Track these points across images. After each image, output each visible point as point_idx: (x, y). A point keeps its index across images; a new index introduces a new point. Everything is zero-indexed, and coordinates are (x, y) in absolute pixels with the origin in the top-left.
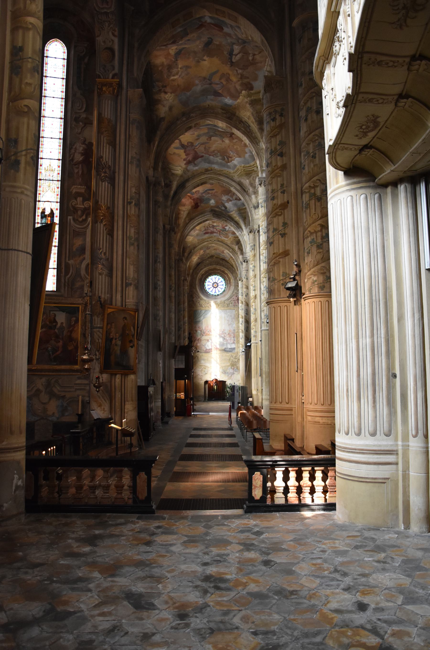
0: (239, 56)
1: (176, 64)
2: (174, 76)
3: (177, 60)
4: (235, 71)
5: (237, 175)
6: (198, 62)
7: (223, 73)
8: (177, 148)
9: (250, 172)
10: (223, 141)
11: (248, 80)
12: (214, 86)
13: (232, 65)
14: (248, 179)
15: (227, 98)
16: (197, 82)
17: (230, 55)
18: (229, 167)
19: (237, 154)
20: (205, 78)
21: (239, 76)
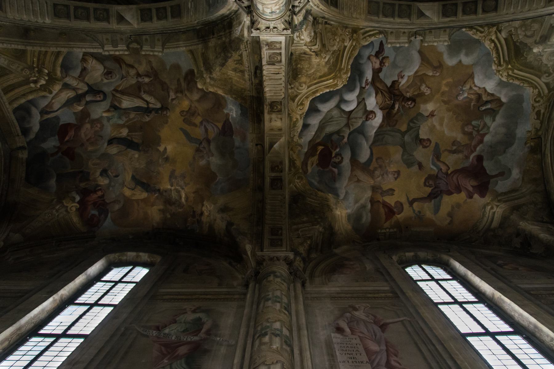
0: (146, 97)
1: (166, 191)
2: (181, 197)
3: (159, 190)
4: (174, 102)
5: (540, 78)
6: (167, 159)
7: (184, 120)
8: (437, 209)
9: (512, 47)
10: (432, 115)
11: (182, 80)
12: (212, 135)
13: (167, 109)
14: (531, 49)
15: (228, 115)
16: (203, 163)
17: (150, 112)
18: (518, 100)
19: (465, 83)
20: (198, 150)
21: (179, 95)
